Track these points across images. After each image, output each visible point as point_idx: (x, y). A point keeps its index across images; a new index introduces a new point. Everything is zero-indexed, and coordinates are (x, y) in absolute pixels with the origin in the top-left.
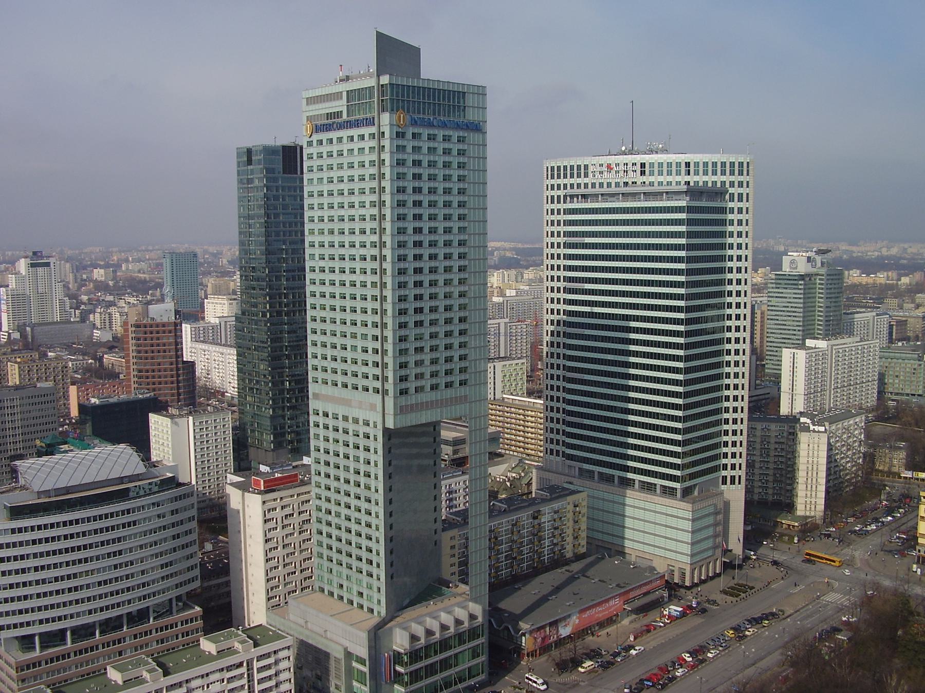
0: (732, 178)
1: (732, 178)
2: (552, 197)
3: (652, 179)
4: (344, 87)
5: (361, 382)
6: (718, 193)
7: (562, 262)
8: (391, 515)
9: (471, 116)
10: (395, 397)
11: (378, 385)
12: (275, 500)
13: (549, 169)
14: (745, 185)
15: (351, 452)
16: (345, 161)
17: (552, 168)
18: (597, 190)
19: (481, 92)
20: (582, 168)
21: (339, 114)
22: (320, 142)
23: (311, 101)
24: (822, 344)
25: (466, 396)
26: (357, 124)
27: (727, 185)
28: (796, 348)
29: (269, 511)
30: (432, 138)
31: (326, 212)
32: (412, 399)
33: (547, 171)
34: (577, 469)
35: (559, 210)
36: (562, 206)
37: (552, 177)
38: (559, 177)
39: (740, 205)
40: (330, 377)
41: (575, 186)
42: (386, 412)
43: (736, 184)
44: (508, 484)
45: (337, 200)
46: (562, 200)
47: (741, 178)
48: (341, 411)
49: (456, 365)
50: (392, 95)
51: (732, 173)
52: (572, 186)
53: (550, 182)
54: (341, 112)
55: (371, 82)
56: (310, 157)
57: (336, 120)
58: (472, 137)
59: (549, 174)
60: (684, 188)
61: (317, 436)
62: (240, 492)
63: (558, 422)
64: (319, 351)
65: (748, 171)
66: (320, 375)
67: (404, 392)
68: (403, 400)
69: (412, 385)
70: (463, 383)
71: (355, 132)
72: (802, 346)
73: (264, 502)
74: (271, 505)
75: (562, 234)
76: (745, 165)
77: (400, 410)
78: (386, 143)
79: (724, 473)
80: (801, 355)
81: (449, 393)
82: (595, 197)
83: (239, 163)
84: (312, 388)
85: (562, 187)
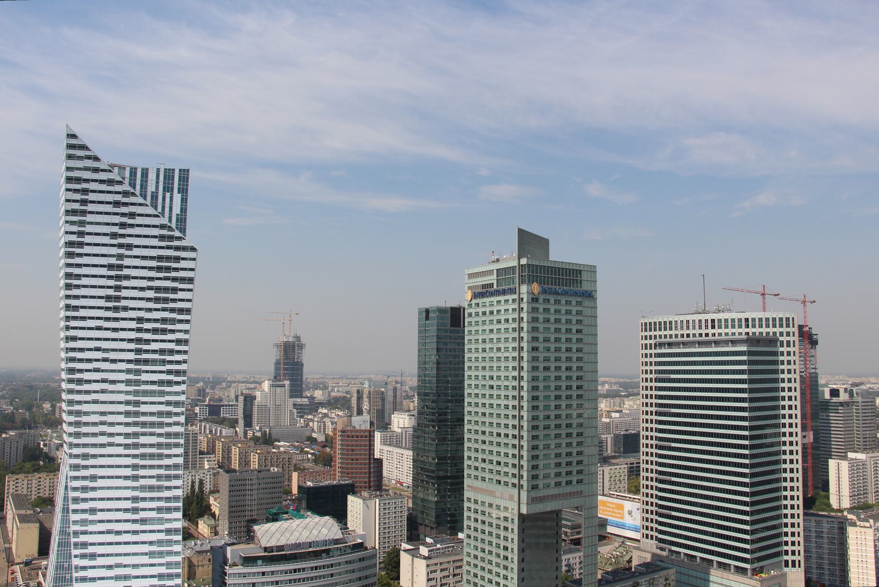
0: (781, 330)
1: (781, 330)
2: (646, 345)
3: (720, 331)
4: (495, 267)
5: (503, 479)
6: (772, 341)
7: (654, 393)
8: (523, 580)
9: (586, 287)
10: (528, 491)
11: (516, 481)
12: (436, 564)
13: (643, 325)
14: (791, 334)
15: (495, 531)
16: (495, 318)
17: (646, 324)
18: (679, 339)
19: (593, 270)
20: (668, 323)
21: (491, 285)
22: (478, 305)
23: (471, 276)
24: (861, 456)
25: (581, 491)
26: (504, 292)
27: (778, 335)
28: (840, 459)
29: (431, 572)
30: (557, 302)
31: (480, 354)
32: (541, 493)
33: (642, 326)
34: (667, 550)
35: (651, 355)
36: (653, 351)
37: (646, 331)
38: (650, 330)
39: (789, 349)
40: (480, 474)
41: (663, 337)
42: (521, 501)
44: (613, 560)
45: (488, 346)
46: (653, 347)
47: (788, 330)
48: (488, 500)
49: (574, 469)
50: (529, 272)
51: (781, 326)
52: (660, 336)
53: (644, 334)
54: (493, 284)
55: (515, 263)
56: (470, 315)
57: (489, 289)
58: (587, 303)
59: (643, 328)
60: (744, 337)
61: (469, 518)
62: (410, 557)
63: (652, 513)
64: (473, 455)
65: (793, 324)
66: (473, 473)
67: (534, 487)
68: (534, 494)
69: (541, 483)
70: (579, 482)
71: (502, 298)
72: (845, 458)
73: (428, 566)
74: (433, 568)
75: (653, 372)
76: (791, 320)
77: (532, 501)
78: (524, 305)
79: (786, 558)
80: (845, 465)
81: (569, 489)
82: (677, 344)
83: (419, 318)
84: (467, 482)
85: (653, 337)
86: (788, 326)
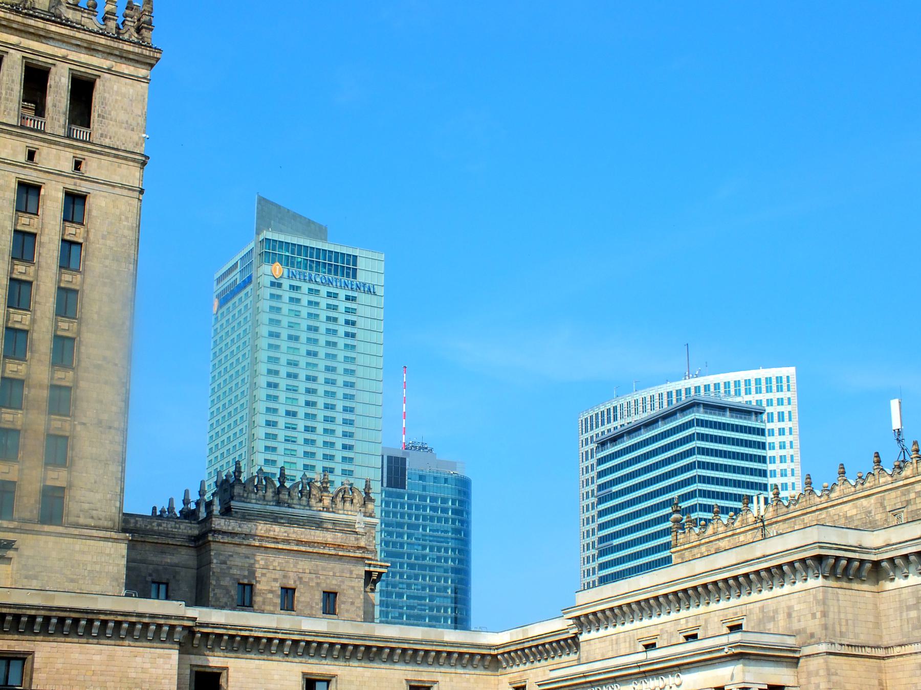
0: (769, 396)
1: (769, 396)
14: (786, 402)
39: (781, 425)
43: (775, 402)
47: (780, 395)
58: (362, 297)
65: (788, 386)
76: (784, 380)
86: (779, 389)
